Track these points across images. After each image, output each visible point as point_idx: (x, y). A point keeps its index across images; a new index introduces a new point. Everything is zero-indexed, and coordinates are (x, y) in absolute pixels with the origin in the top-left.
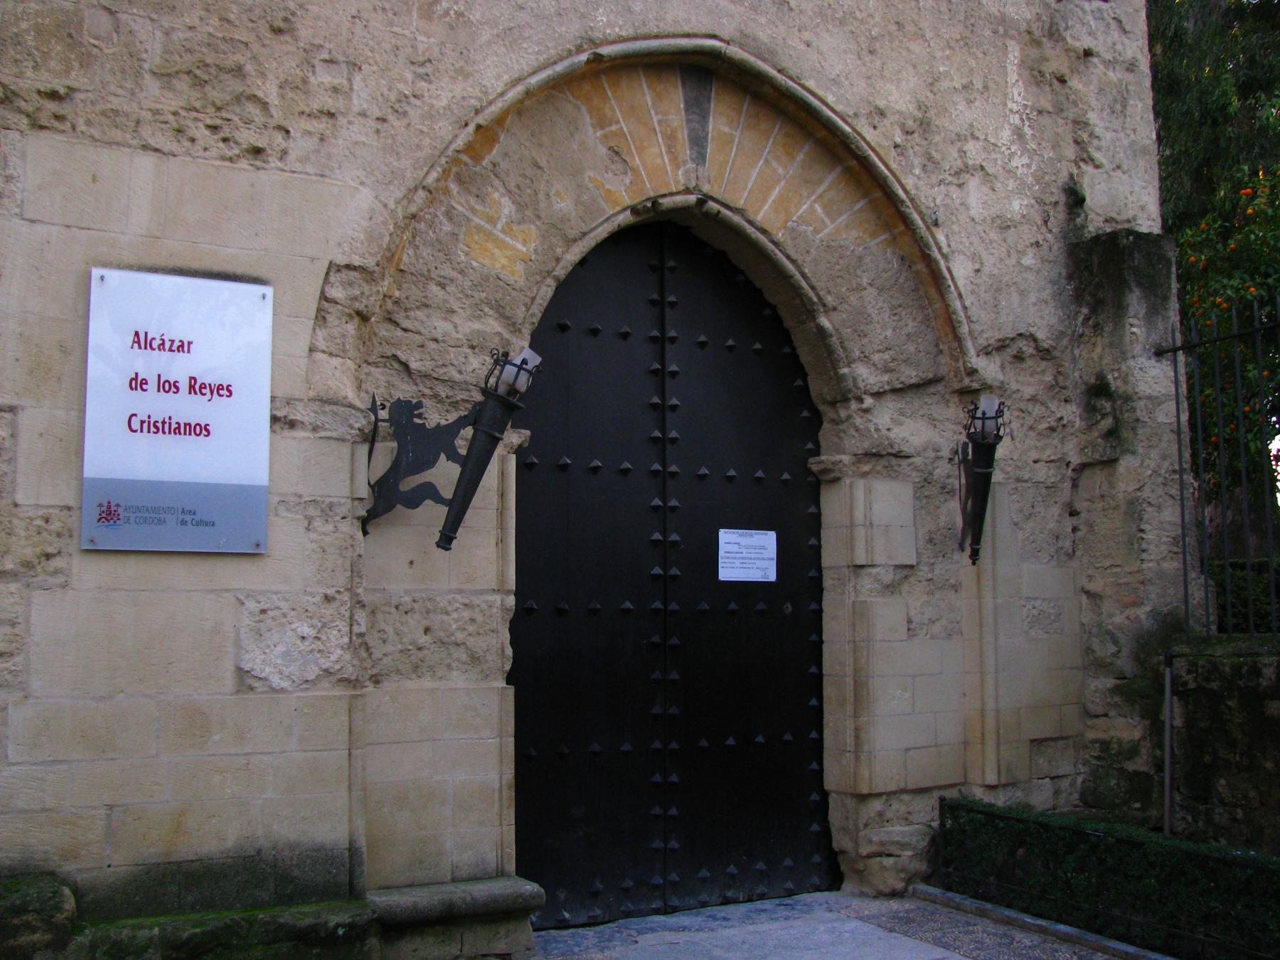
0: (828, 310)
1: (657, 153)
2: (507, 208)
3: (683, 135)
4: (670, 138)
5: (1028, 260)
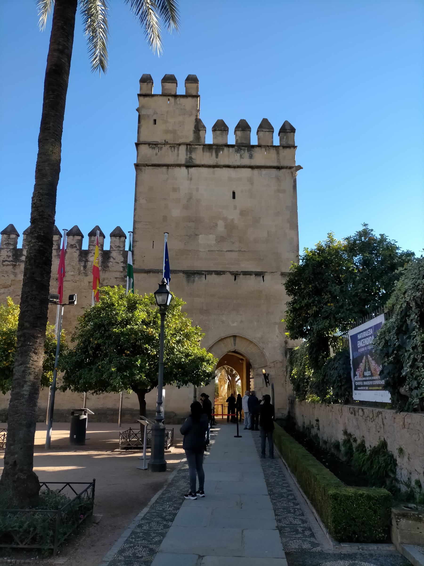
3: (233, 344)
5: (279, 351)
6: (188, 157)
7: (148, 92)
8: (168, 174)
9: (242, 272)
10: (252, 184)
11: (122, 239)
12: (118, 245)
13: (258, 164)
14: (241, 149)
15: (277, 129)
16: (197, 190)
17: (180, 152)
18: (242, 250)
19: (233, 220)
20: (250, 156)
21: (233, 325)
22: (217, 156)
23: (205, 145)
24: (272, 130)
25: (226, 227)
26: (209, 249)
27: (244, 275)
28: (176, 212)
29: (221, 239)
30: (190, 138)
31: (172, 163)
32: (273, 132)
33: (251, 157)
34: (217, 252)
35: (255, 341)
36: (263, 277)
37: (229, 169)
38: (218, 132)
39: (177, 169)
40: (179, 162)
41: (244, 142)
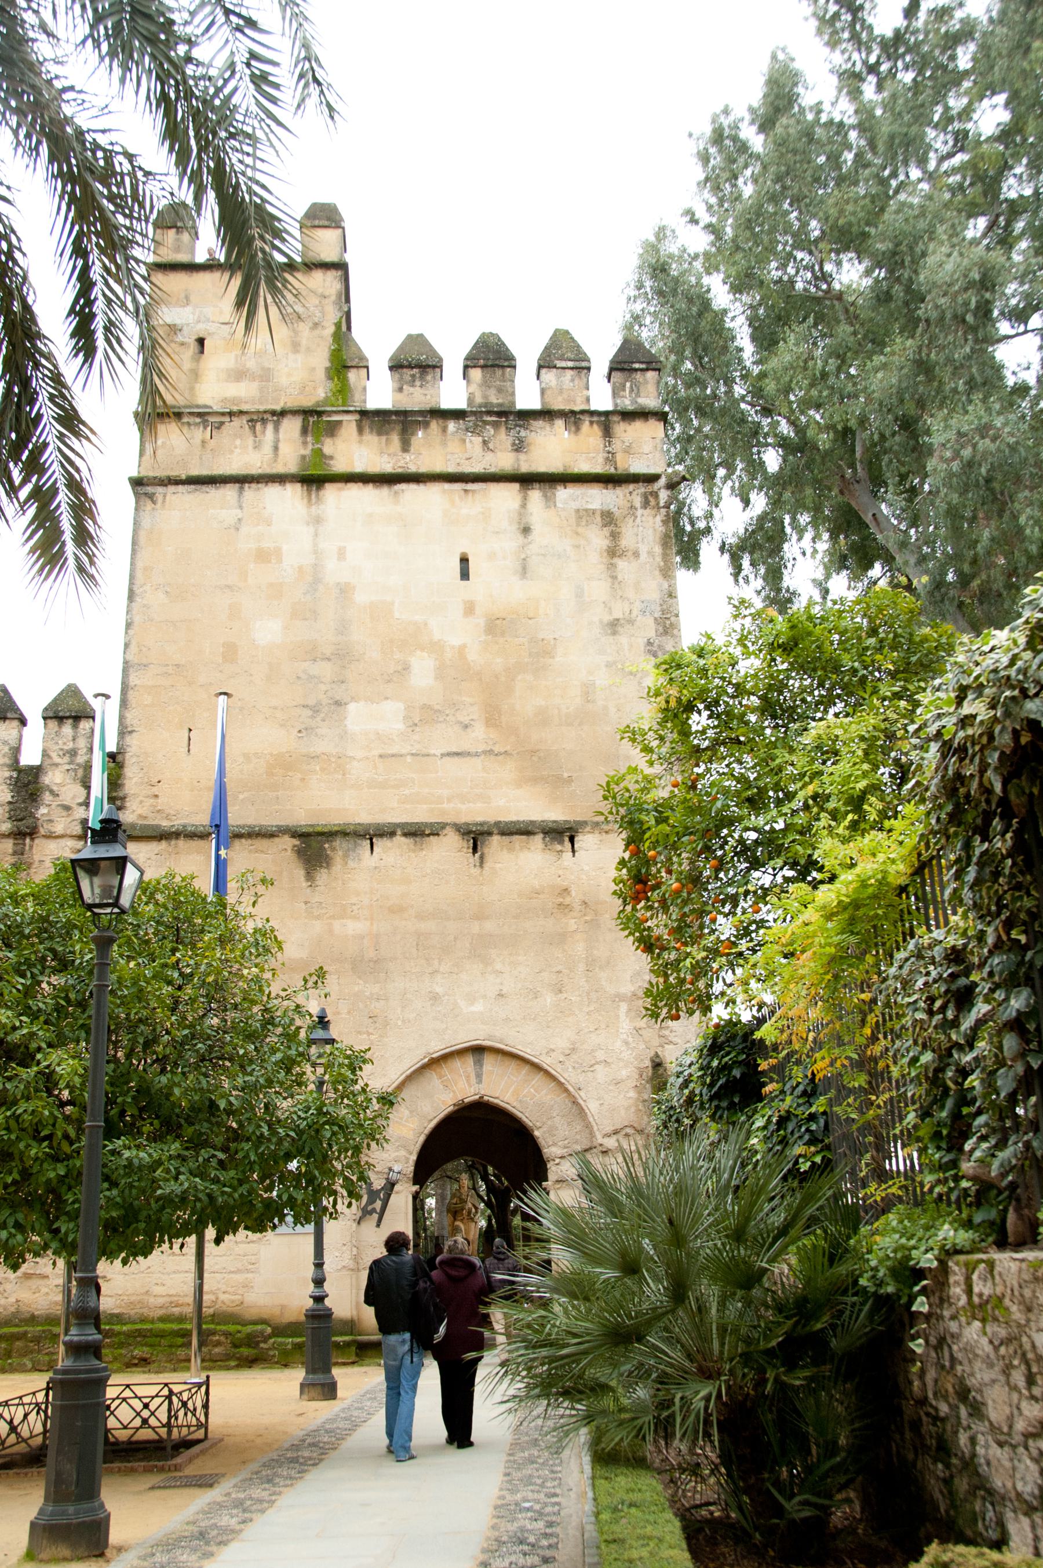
0: (539, 1128)
1: (462, 1083)
2: (407, 1112)
3: (473, 1076)
4: (468, 1077)
6: (307, 452)
7: (183, 258)
8: (241, 507)
9: (497, 824)
10: (526, 530)
11: (85, 725)
12: (71, 745)
13: (542, 468)
14: (486, 423)
15: (600, 361)
16: (341, 554)
17: (282, 435)
18: (496, 749)
19: (462, 649)
20: (514, 444)
21: (473, 1009)
22: (406, 447)
23: (364, 413)
24: (584, 364)
25: (440, 673)
26: (381, 751)
27: (503, 833)
28: (268, 631)
29: (423, 716)
30: (319, 392)
31: (254, 471)
32: (589, 369)
33: (519, 447)
34: (409, 759)
35: (548, 1060)
36: (572, 840)
37: (447, 486)
38: (407, 373)
39: (273, 491)
40: (280, 469)
41: (495, 399)
